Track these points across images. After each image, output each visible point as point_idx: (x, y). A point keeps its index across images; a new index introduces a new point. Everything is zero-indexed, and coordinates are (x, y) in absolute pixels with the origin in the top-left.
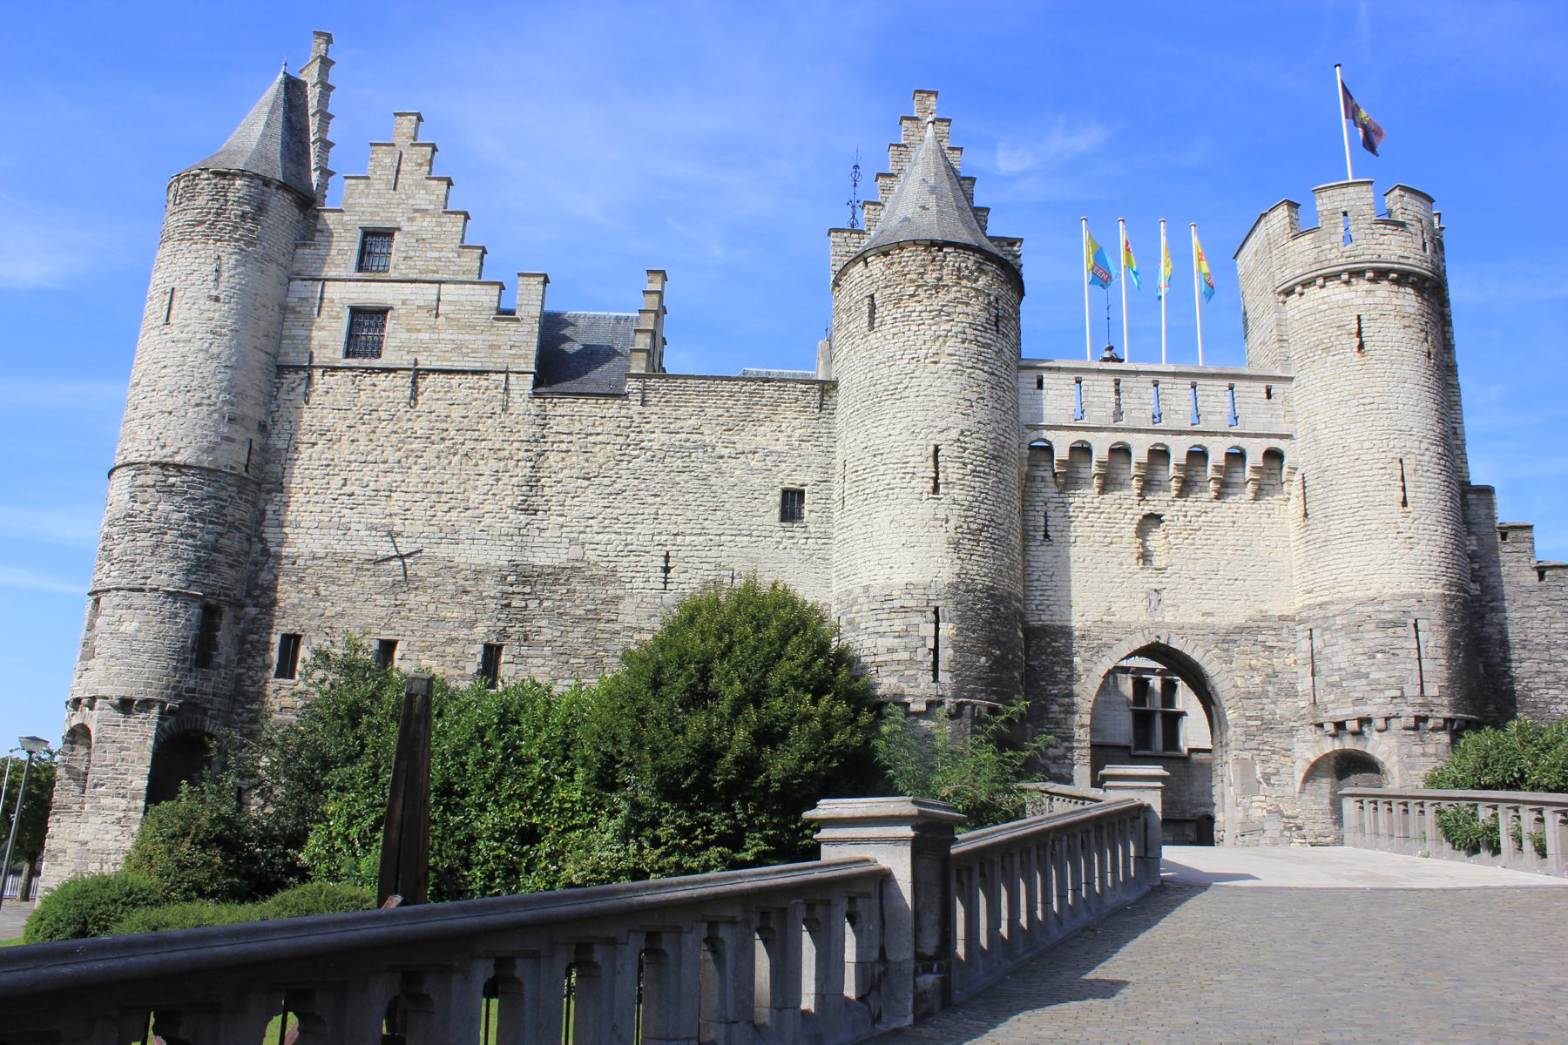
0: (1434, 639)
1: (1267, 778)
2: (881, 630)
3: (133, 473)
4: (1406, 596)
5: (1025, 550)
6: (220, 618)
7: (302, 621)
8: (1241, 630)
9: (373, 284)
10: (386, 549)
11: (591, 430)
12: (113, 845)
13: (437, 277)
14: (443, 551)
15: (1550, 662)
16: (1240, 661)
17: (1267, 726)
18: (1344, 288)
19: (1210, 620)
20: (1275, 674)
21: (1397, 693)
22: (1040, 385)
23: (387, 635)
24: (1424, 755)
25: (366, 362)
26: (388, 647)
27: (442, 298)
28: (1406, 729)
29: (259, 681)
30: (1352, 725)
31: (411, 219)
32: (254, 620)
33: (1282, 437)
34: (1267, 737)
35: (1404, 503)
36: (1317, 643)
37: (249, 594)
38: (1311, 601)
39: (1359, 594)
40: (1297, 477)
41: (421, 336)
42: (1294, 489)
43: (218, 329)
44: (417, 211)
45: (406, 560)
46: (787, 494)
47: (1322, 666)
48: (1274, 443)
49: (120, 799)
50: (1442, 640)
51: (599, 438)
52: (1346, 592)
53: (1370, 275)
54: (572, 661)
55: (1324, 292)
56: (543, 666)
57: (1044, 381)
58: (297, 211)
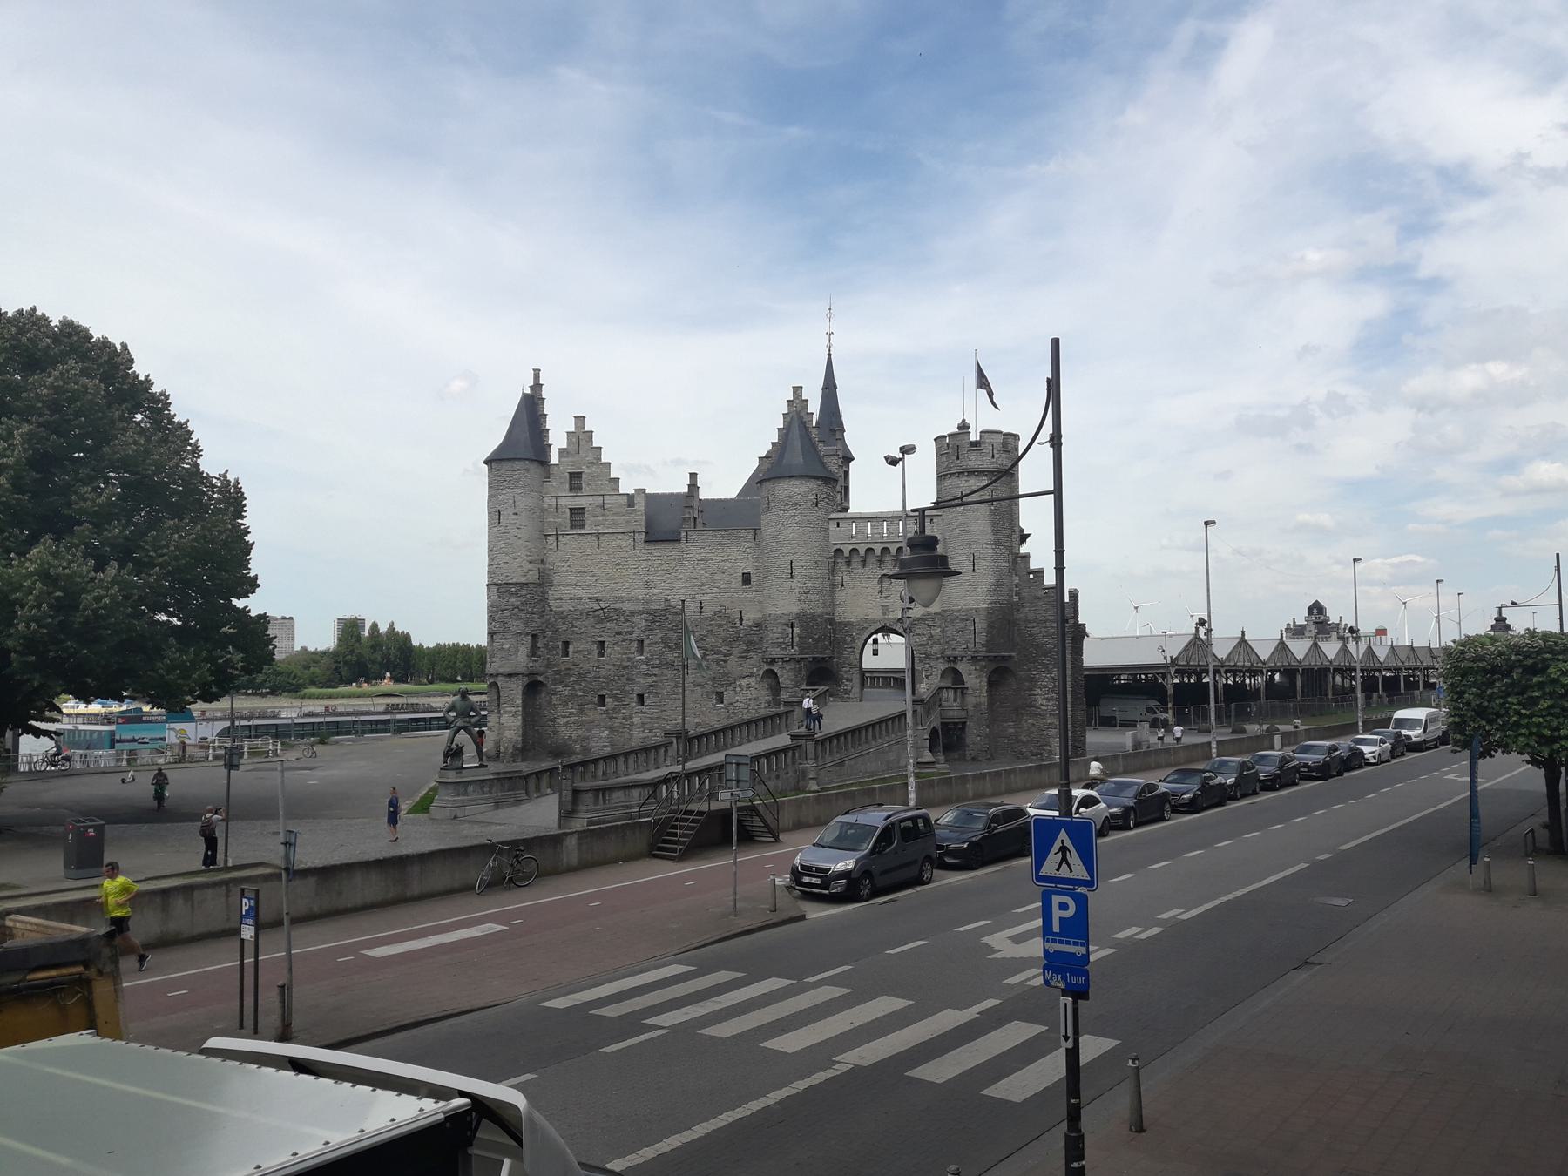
0: (981, 625)
1: (927, 677)
4: (971, 609)
5: (832, 593)
8: (918, 619)
10: (596, 607)
13: (602, 493)
14: (618, 606)
15: (1045, 627)
17: (928, 656)
20: (932, 636)
21: (965, 647)
22: (838, 526)
24: (976, 669)
28: (969, 660)
34: (928, 661)
35: (974, 570)
50: (985, 625)
51: (671, 558)
58: (540, 467)
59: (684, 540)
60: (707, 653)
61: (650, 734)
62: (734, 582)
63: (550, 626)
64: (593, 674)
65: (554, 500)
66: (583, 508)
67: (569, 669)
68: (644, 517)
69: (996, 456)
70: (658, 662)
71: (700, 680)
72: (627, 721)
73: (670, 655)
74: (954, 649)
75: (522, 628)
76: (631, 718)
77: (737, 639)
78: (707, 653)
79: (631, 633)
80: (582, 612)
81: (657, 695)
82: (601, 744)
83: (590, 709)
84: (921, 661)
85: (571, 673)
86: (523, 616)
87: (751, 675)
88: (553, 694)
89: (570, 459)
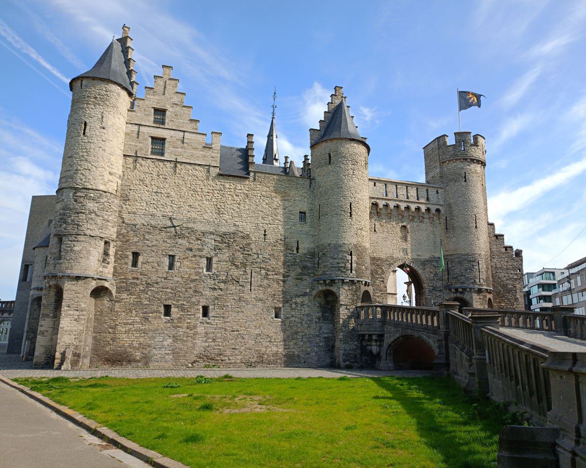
2: (335, 257)
3: (74, 191)
6: (109, 246)
7: (139, 247)
8: (427, 261)
9: (159, 129)
10: (170, 224)
11: (240, 188)
12: (75, 328)
14: (190, 225)
16: (427, 270)
17: (434, 289)
18: (461, 163)
19: (420, 257)
21: (473, 281)
23: (171, 253)
24: (480, 299)
25: (158, 157)
26: (172, 257)
27: (185, 137)
29: (123, 268)
30: (460, 290)
31: (173, 107)
32: (120, 247)
33: (441, 205)
35: (476, 227)
36: (450, 266)
37: (117, 237)
38: (448, 254)
39: (462, 253)
40: (444, 218)
41: (178, 150)
42: (443, 221)
43: (104, 139)
44: (174, 104)
45: (177, 228)
46: (300, 212)
47: (451, 272)
48: (438, 207)
49: (77, 312)
52: (459, 252)
53: (469, 160)
54: (236, 263)
55: (455, 164)
56: (226, 265)
57: (376, 184)
59: (251, 179)
60: (269, 273)
61: (213, 344)
62: (292, 217)
63: (121, 237)
64: (161, 285)
65: (137, 127)
66: (164, 139)
67: (138, 279)
68: (219, 155)
69: (484, 153)
70: (224, 278)
71: (262, 296)
72: (191, 330)
73: (235, 272)
74: (463, 283)
75: (97, 233)
76: (195, 327)
77: (294, 264)
78: (269, 273)
79: (200, 250)
80: (154, 227)
81: (222, 307)
82: (163, 351)
83: (155, 318)
84: (430, 292)
85: (138, 282)
86: (99, 222)
87: (305, 294)
88: (116, 302)
89: (156, 97)
